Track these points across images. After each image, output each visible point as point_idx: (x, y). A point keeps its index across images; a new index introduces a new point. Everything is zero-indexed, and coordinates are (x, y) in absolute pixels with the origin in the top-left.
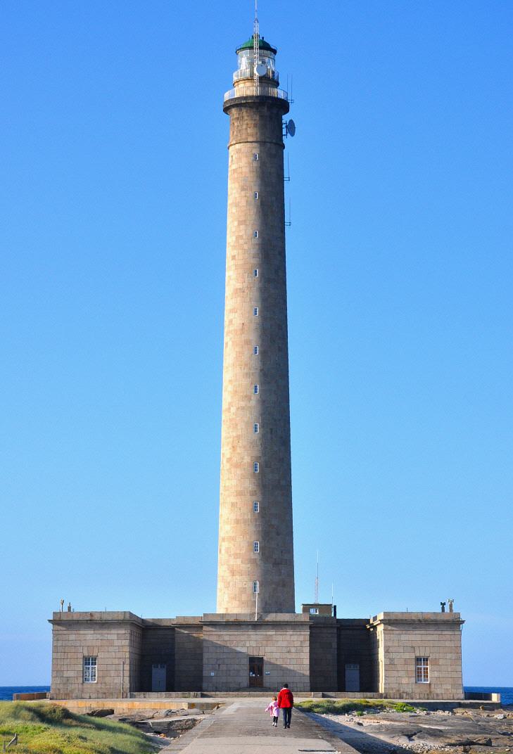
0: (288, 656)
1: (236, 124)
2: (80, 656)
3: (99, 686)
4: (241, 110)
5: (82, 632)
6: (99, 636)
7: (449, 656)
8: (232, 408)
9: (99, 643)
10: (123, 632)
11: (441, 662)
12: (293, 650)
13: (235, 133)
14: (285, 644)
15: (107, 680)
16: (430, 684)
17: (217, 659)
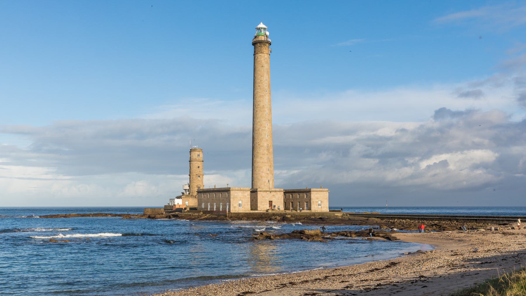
0: (279, 200)
1: (259, 48)
2: (238, 200)
3: (243, 209)
4: (261, 44)
5: (238, 193)
6: (243, 195)
7: (326, 200)
8: (260, 130)
9: (243, 196)
10: (249, 193)
11: (324, 202)
12: (280, 199)
13: (259, 50)
14: (277, 197)
15: (245, 207)
16: (321, 208)
17: (261, 201)
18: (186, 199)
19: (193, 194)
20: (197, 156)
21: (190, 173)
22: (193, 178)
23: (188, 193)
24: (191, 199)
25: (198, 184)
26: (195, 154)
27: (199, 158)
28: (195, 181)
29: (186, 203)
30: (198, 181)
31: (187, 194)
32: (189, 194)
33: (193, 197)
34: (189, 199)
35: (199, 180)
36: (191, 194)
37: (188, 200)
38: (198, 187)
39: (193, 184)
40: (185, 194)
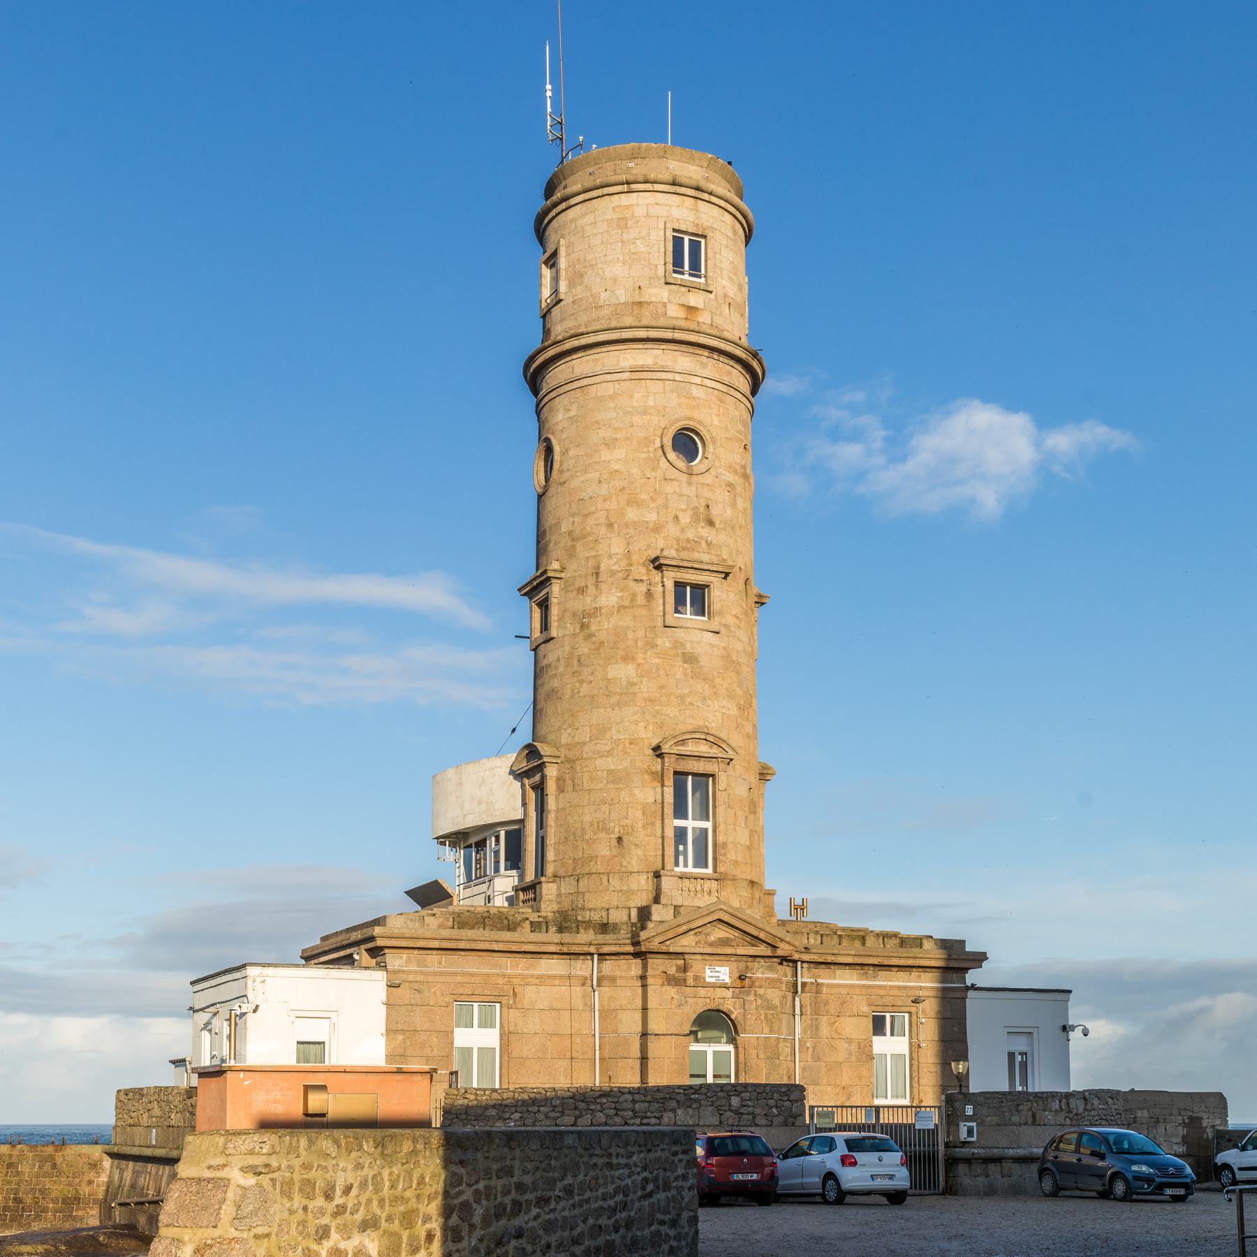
18: (471, 965)
19: (594, 901)
20: (660, 255)
21: (541, 550)
22: (584, 621)
23: (505, 883)
24: (555, 966)
25: (679, 718)
26: (622, 223)
27: (695, 299)
28: (621, 672)
29: (464, 1037)
30: (679, 669)
31: (500, 902)
32: (530, 889)
33: (585, 936)
34: (512, 967)
35: (690, 659)
36: (548, 890)
37: (507, 996)
38: (680, 775)
39: (597, 716)
40: (464, 897)
